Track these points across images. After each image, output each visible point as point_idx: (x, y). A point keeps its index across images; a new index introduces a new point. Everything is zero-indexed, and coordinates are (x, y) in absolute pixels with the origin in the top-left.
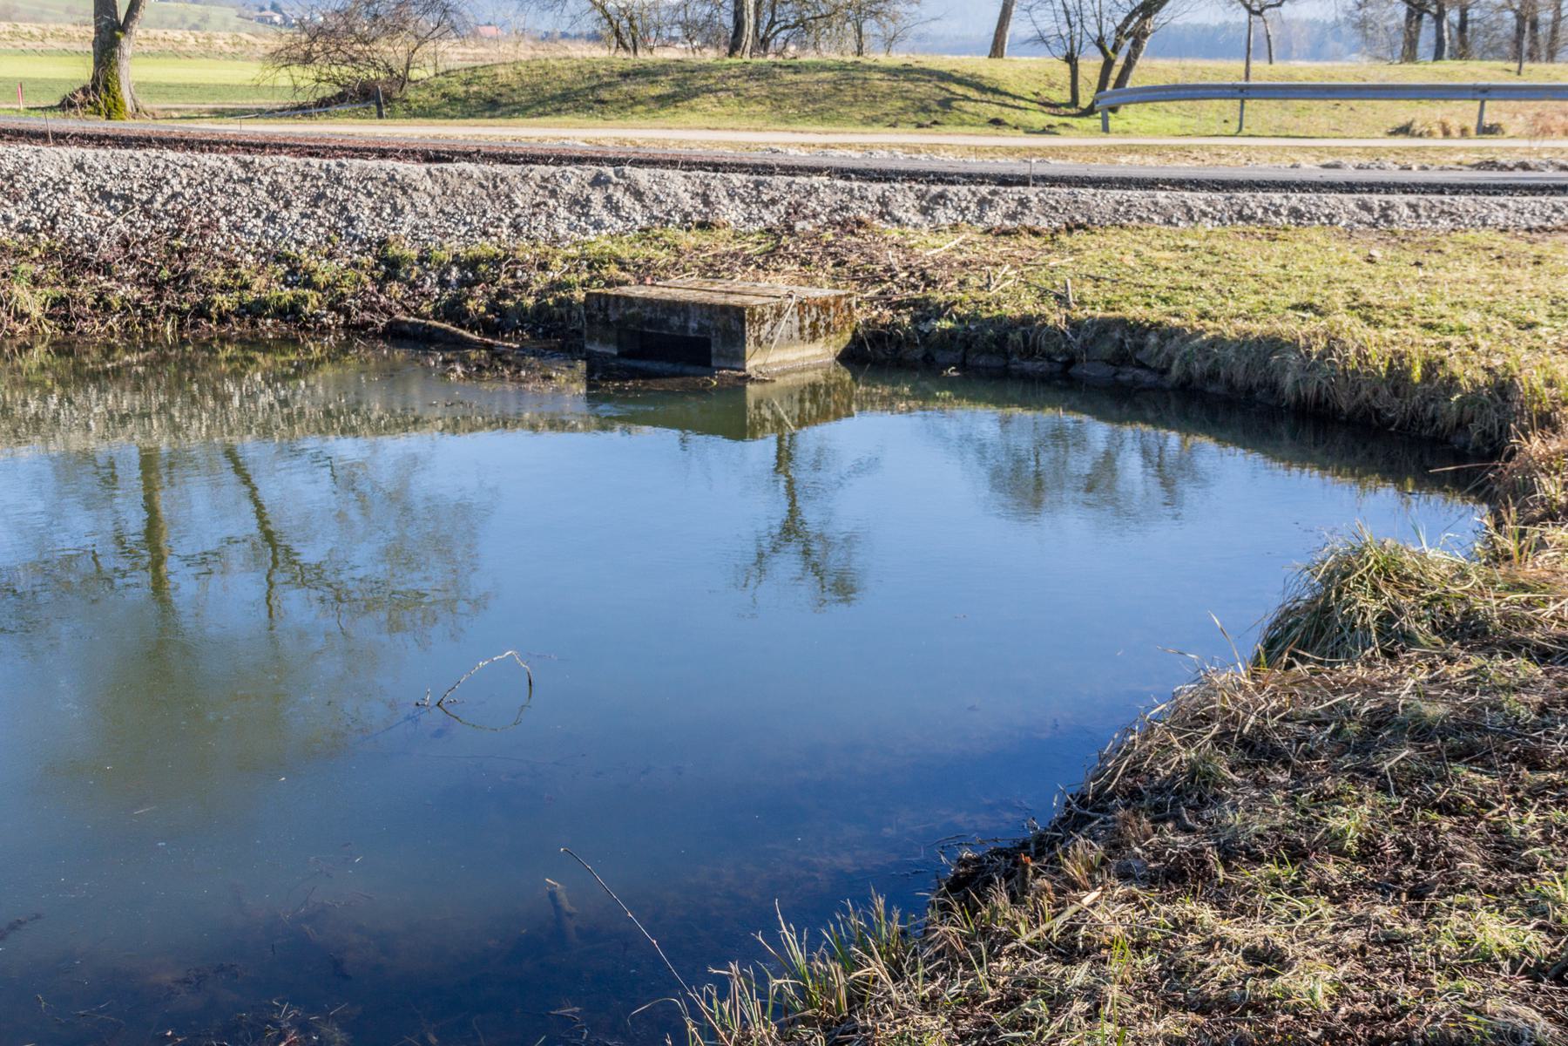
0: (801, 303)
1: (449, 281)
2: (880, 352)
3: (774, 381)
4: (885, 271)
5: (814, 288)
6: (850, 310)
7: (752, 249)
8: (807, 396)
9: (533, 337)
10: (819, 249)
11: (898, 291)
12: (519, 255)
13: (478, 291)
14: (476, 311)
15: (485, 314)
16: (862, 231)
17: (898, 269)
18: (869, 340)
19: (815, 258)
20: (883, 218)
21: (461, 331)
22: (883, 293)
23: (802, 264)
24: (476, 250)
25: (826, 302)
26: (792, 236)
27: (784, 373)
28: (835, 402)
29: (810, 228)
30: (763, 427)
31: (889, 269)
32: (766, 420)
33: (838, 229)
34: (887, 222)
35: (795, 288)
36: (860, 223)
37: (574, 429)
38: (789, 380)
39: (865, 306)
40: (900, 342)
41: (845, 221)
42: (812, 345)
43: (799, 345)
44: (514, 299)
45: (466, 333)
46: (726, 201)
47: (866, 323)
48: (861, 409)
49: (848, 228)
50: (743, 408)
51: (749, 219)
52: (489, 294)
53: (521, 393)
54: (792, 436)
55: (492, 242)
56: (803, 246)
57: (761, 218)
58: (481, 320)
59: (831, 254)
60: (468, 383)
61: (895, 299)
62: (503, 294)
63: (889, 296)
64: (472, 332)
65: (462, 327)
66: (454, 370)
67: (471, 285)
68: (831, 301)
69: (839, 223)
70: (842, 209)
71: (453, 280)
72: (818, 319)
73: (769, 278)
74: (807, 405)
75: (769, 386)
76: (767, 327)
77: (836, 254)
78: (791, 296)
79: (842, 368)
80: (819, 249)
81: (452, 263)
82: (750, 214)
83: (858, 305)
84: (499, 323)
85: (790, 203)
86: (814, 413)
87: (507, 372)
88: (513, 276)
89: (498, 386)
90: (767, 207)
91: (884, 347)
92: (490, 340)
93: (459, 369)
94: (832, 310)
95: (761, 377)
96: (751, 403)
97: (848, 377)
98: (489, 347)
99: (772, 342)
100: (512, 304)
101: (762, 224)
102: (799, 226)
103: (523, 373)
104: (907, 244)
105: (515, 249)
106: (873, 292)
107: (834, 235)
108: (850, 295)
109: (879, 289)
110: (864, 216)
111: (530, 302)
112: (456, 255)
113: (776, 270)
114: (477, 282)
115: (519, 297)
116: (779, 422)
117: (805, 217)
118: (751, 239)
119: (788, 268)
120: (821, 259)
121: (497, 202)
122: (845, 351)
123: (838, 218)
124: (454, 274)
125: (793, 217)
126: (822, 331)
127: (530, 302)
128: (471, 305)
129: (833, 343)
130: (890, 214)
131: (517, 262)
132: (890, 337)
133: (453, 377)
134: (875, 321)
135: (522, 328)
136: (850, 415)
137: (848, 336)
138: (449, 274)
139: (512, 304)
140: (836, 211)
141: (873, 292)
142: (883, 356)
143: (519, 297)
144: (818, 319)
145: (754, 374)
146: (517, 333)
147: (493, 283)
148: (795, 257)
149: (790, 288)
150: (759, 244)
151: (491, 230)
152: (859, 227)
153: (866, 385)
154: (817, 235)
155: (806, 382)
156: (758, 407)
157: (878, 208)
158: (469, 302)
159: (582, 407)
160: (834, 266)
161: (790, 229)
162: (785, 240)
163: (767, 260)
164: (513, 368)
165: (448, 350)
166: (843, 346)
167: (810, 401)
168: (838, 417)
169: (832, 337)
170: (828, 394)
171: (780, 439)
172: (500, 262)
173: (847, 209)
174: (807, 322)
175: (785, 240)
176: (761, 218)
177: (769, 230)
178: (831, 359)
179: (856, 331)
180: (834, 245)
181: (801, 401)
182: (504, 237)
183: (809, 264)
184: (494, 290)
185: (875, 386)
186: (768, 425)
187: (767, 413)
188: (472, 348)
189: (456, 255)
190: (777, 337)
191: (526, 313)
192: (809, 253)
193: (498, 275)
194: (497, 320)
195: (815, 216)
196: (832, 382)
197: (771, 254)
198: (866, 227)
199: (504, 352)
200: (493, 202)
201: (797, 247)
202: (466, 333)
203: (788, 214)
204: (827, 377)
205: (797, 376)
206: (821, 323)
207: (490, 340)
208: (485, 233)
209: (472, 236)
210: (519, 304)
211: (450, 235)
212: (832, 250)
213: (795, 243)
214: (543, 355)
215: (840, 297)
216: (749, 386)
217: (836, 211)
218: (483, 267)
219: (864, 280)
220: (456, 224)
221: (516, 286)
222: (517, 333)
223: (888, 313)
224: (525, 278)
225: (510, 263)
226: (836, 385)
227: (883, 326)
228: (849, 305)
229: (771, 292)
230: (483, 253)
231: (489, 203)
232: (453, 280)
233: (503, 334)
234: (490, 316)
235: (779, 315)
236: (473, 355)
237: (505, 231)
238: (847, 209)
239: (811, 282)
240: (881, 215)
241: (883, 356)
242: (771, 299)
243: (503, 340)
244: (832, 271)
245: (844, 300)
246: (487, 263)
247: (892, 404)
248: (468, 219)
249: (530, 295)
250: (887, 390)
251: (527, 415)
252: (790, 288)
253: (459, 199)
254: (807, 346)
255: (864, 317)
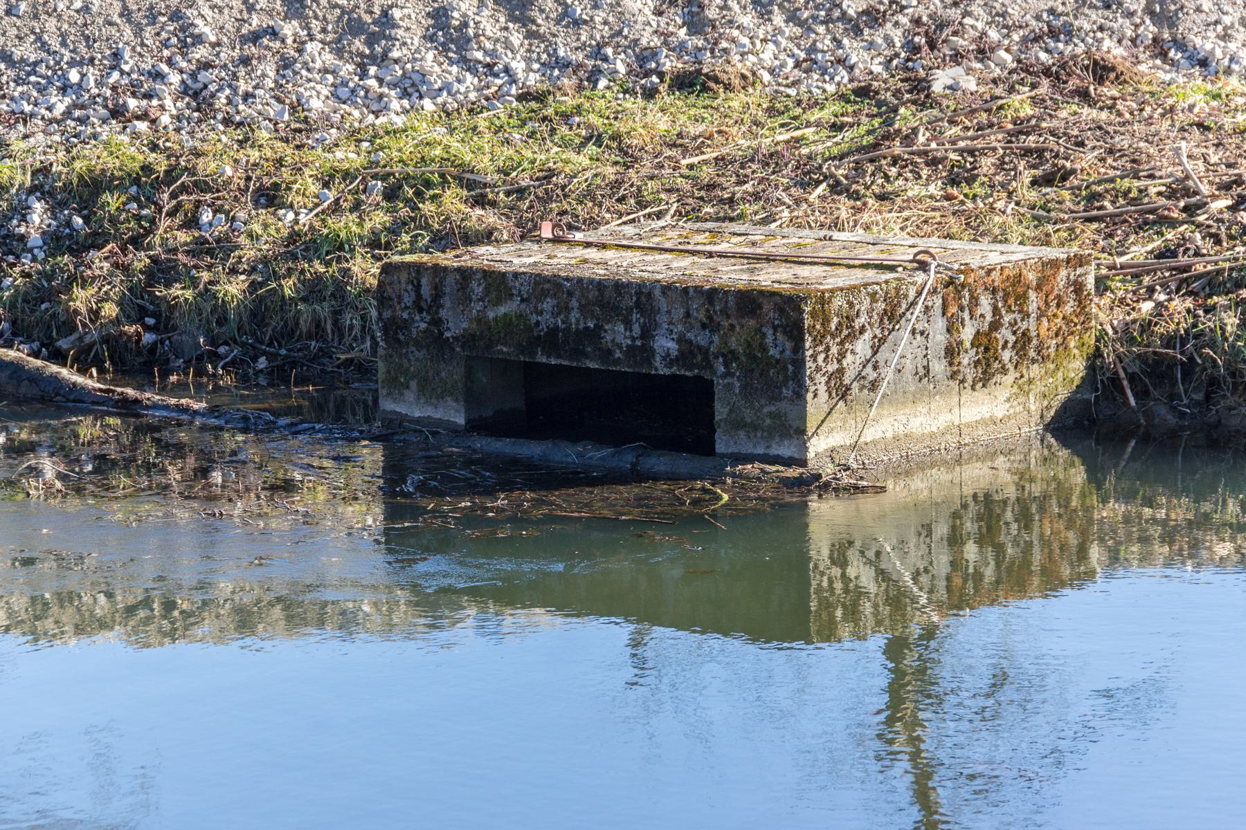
0: (950, 282)
1: (22, 238)
2: (1162, 410)
3: (883, 489)
4: (1172, 194)
5: (985, 245)
6: (1082, 303)
7: (818, 143)
8: (969, 526)
9: (244, 380)
10: (996, 139)
11: (1207, 246)
12: (206, 167)
13: (98, 261)
14: (95, 314)
15: (117, 322)
16: (1109, 91)
17: (1205, 189)
18: (1132, 378)
19: (987, 164)
20: (1163, 55)
21: (54, 368)
22: (1166, 253)
23: (954, 181)
24: (92, 158)
25: (1018, 279)
26: (923, 106)
27: (907, 467)
28: (1045, 543)
29: (970, 84)
30: (853, 613)
31: (1180, 189)
32: (859, 593)
33: (1045, 88)
34: (1173, 63)
35: (933, 243)
36: (1101, 71)
37: (348, 622)
38: (920, 485)
39: (1120, 288)
40: (1214, 382)
41: (1063, 66)
42: (980, 394)
43: (946, 393)
44: (194, 282)
45: (67, 374)
46: (747, 20)
47: (1125, 335)
48: (1114, 558)
49: (1073, 83)
50: (800, 562)
51: (808, 64)
52: (126, 269)
53: (212, 527)
54: (930, 632)
55: (136, 135)
56: (955, 131)
57: (841, 61)
58: (106, 340)
59: (1027, 152)
60: (74, 503)
61: (1200, 268)
62: (162, 271)
63: (1183, 260)
64: (83, 371)
65: (58, 357)
66: (35, 472)
67: (79, 247)
68: (1031, 277)
69: (1047, 72)
70: (1053, 34)
71: (35, 238)
72: (995, 325)
73: (865, 217)
74: (971, 551)
75: (867, 504)
76: (862, 347)
77: (1040, 152)
78: (923, 266)
79: (1064, 453)
80: (996, 139)
81: (31, 191)
82: (813, 49)
83: (1102, 285)
84: (153, 348)
85: (917, 22)
86: (989, 573)
87: (174, 475)
88: (192, 222)
89: (149, 509)
90: (857, 31)
91: (1173, 396)
92: (130, 392)
93: (49, 467)
94: (1034, 301)
95: (846, 480)
96: (820, 545)
97: (1078, 476)
98: (128, 408)
99: (874, 386)
100: (189, 294)
101: (842, 76)
102: (941, 81)
103: (217, 477)
104: (1227, 121)
105: (197, 154)
106: (1139, 251)
107: (1035, 101)
108: (1080, 261)
109: (1157, 243)
110: (1113, 51)
111: (234, 289)
112: (44, 170)
113: (882, 197)
114: (96, 241)
115: (205, 276)
116: (897, 600)
117: (957, 57)
118: (814, 115)
119: (915, 190)
120: (1001, 165)
121: (149, 32)
122: (1065, 407)
123: (1043, 56)
124: (36, 218)
125: (927, 59)
126: (1006, 355)
127: (234, 289)
128: (81, 299)
129: (1038, 387)
130: (1181, 45)
131: (202, 186)
132: (1189, 368)
133: (34, 488)
134: (1146, 326)
135: (214, 357)
136: (1084, 577)
137: (1076, 367)
138: (24, 219)
139: (189, 294)
140: (1037, 39)
141: (1139, 251)
142: (1172, 420)
143: (205, 276)
144: (995, 325)
145: (828, 471)
146: (200, 372)
147: (137, 242)
148: (933, 162)
149: (922, 244)
150: (837, 127)
151: (132, 103)
152: (1100, 81)
153: (1128, 496)
154: (991, 105)
155: (968, 491)
156: (839, 558)
157: (1149, 30)
158: (78, 292)
159: (374, 563)
160: (1035, 183)
161: (919, 88)
162: (906, 117)
163: (858, 168)
164: (191, 462)
165: (20, 418)
166: (1063, 394)
167: (980, 542)
168: (1052, 583)
169: (1035, 370)
170: (1025, 519)
171: (895, 649)
172: (157, 185)
173: (1069, 33)
174: (967, 334)
175: (906, 117)
176: (841, 61)
177: (863, 92)
178: (1032, 428)
179: (1098, 353)
180: (1036, 130)
181: (955, 540)
182: (165, 119)
183: (970, 181)
184: (140, 261)
185: (1150, 502)
186: (867, 608)
187: (865, 577)
188: (85, 412)
189: (44, 170)
190: (889, 374)
191: (224, 320)
192: (972, 152)
193: (153, 221)
194: (148, 338)
195: (983, 53)
196: (1036, 489)
197: (870, 151)
198: (1119, 80)
199: (163, 425)
200: (138, 31)
201: (936, 135)
202: (67, 374)
203: (916, 49)
204: (1023, 477)
205: (941, 475)
206: (1005, 334)
207: (130, 392)
208: (118, 113)
209: (82, 121)
210: (207, 293)
211: (26, 118)
212: (1031, 141)
213: (931, 124)
214: (270, 428)
215: (1054, 264)
216: (814, 504)
217: (1037, 39)
218: (112, 201)
219: (1115, 220)
220: (42, 90)
221: (200, 248)
222: (200, 372)
223: (1180, 305)
224: (222, 228)
225: (184, 189)
226: (1045, 497)
227: (1169, 341)
228: (1078, 287)
229: (873, 254)
230: (111, 163)
231: (128, 32)
232: (35, 238)
233: (165, 374)
234: (131, 329)
235: (892, 316)
236: (87, 429)
237: (169, 107)
238: (1069, 33)
239: (975, 228)
240: (1159, 50)
241: (1172, 420)
242: (871, 274)
243: (162, 390)
244: (1033, 196)
245: (1063, 273)
246: (121, 188)
247: (1195, 545)
248: (74, 76)
249: (234, 271)
250: (1180, 511)
251: (225, 587)
252: (922, 244)
253: (51, 24)
254: (967, 395)
255: (1119, 316)
